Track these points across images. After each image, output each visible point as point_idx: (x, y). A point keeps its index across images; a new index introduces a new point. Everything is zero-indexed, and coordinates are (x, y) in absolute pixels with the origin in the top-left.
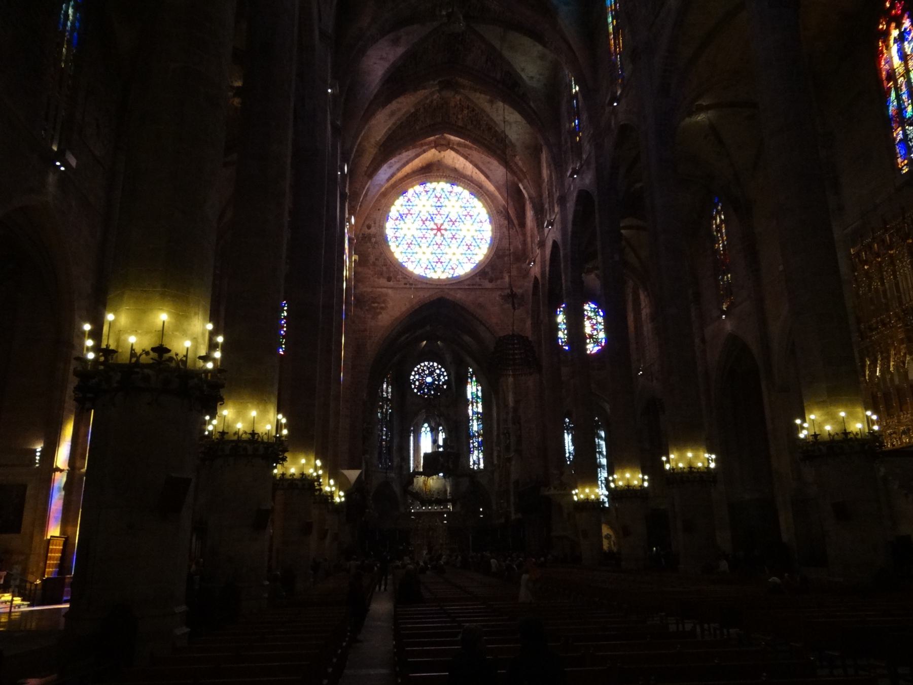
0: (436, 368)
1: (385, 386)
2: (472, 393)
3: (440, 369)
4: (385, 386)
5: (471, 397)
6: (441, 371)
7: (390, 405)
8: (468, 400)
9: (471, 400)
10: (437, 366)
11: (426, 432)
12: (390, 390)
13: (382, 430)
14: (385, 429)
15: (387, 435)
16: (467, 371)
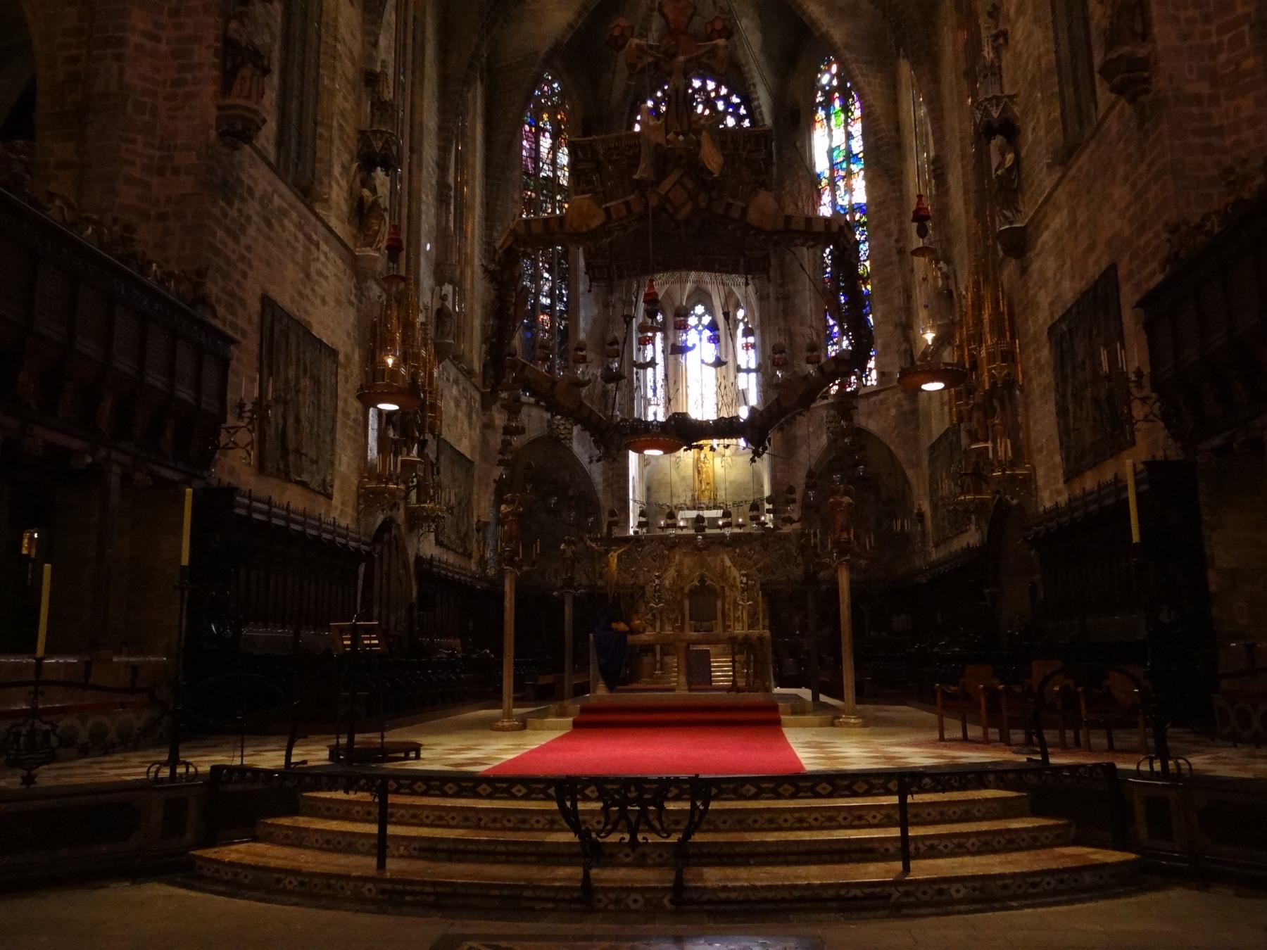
0: (713, 95)
1: (546, 143)
2: (831, 151)
3: (726, 99)
4: (546, 143)
5: (827, 165)
6: (728, 103)
7: (566, 206)
8: (816, 179)
9: (827, 174)
10: (717, 90)
11: (700, 328)
12: (563, 159)
13: (536, 278)
14: (546, 275)
15: (551, 294)
16: (813, 86)
